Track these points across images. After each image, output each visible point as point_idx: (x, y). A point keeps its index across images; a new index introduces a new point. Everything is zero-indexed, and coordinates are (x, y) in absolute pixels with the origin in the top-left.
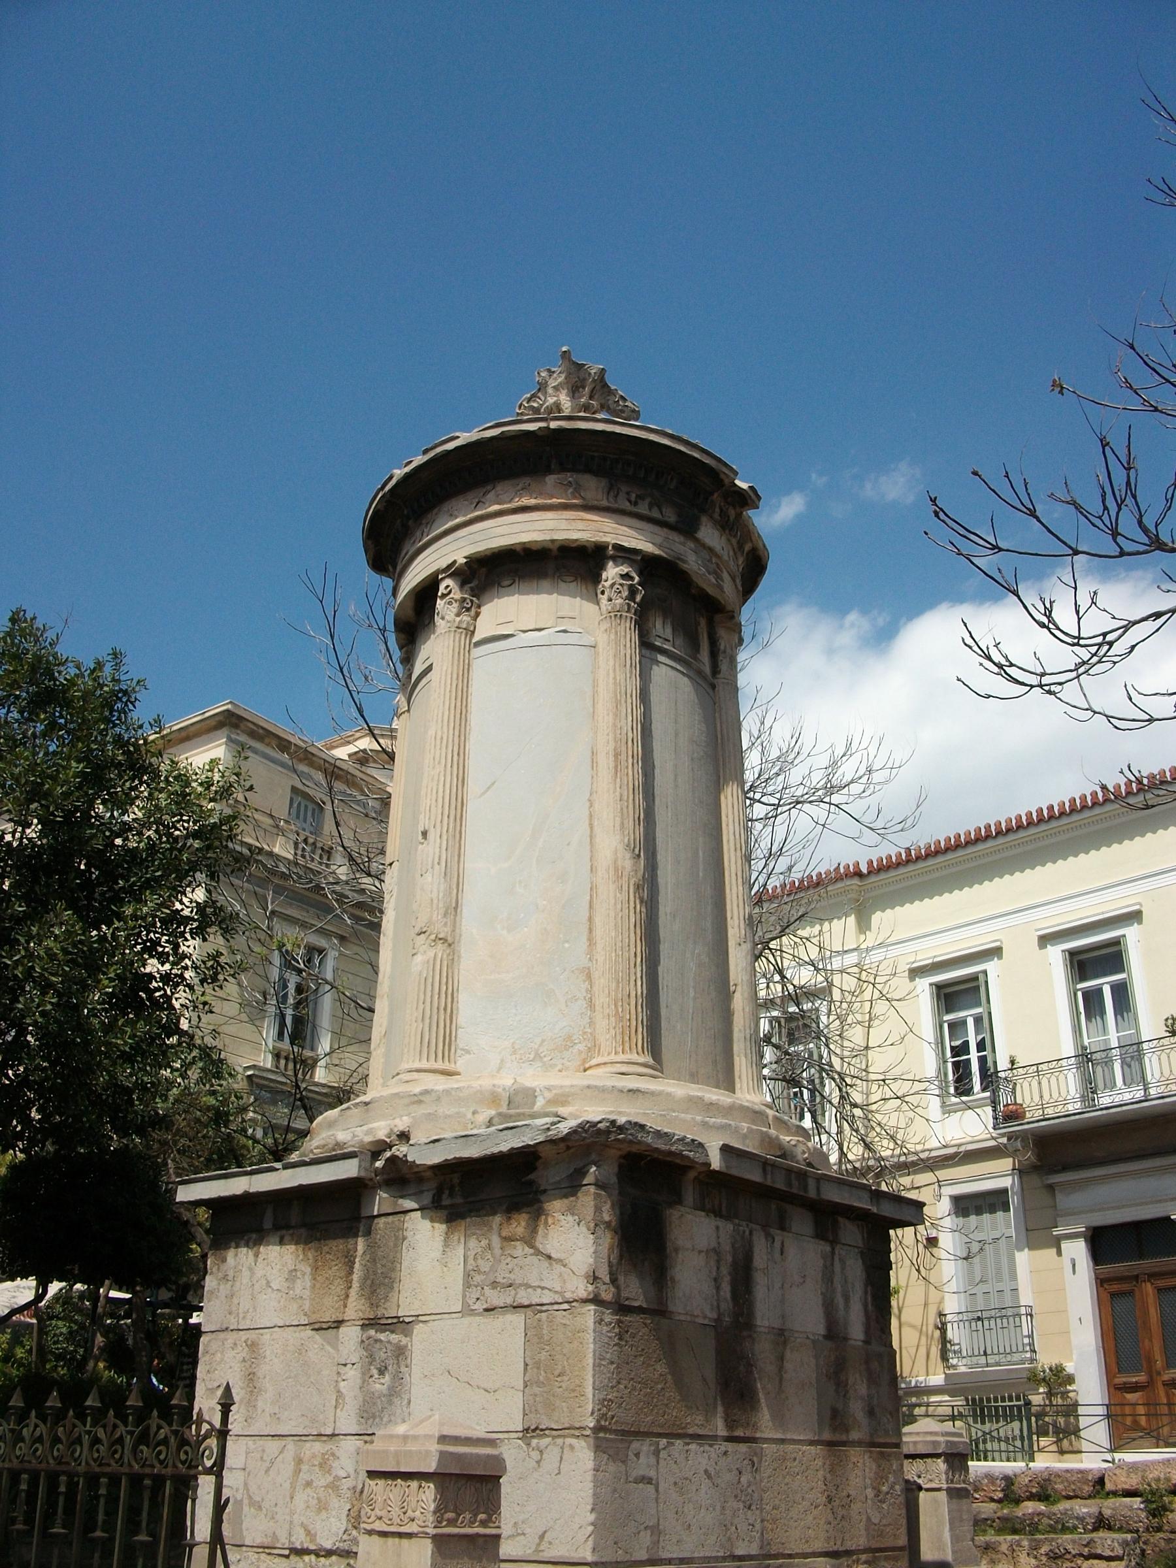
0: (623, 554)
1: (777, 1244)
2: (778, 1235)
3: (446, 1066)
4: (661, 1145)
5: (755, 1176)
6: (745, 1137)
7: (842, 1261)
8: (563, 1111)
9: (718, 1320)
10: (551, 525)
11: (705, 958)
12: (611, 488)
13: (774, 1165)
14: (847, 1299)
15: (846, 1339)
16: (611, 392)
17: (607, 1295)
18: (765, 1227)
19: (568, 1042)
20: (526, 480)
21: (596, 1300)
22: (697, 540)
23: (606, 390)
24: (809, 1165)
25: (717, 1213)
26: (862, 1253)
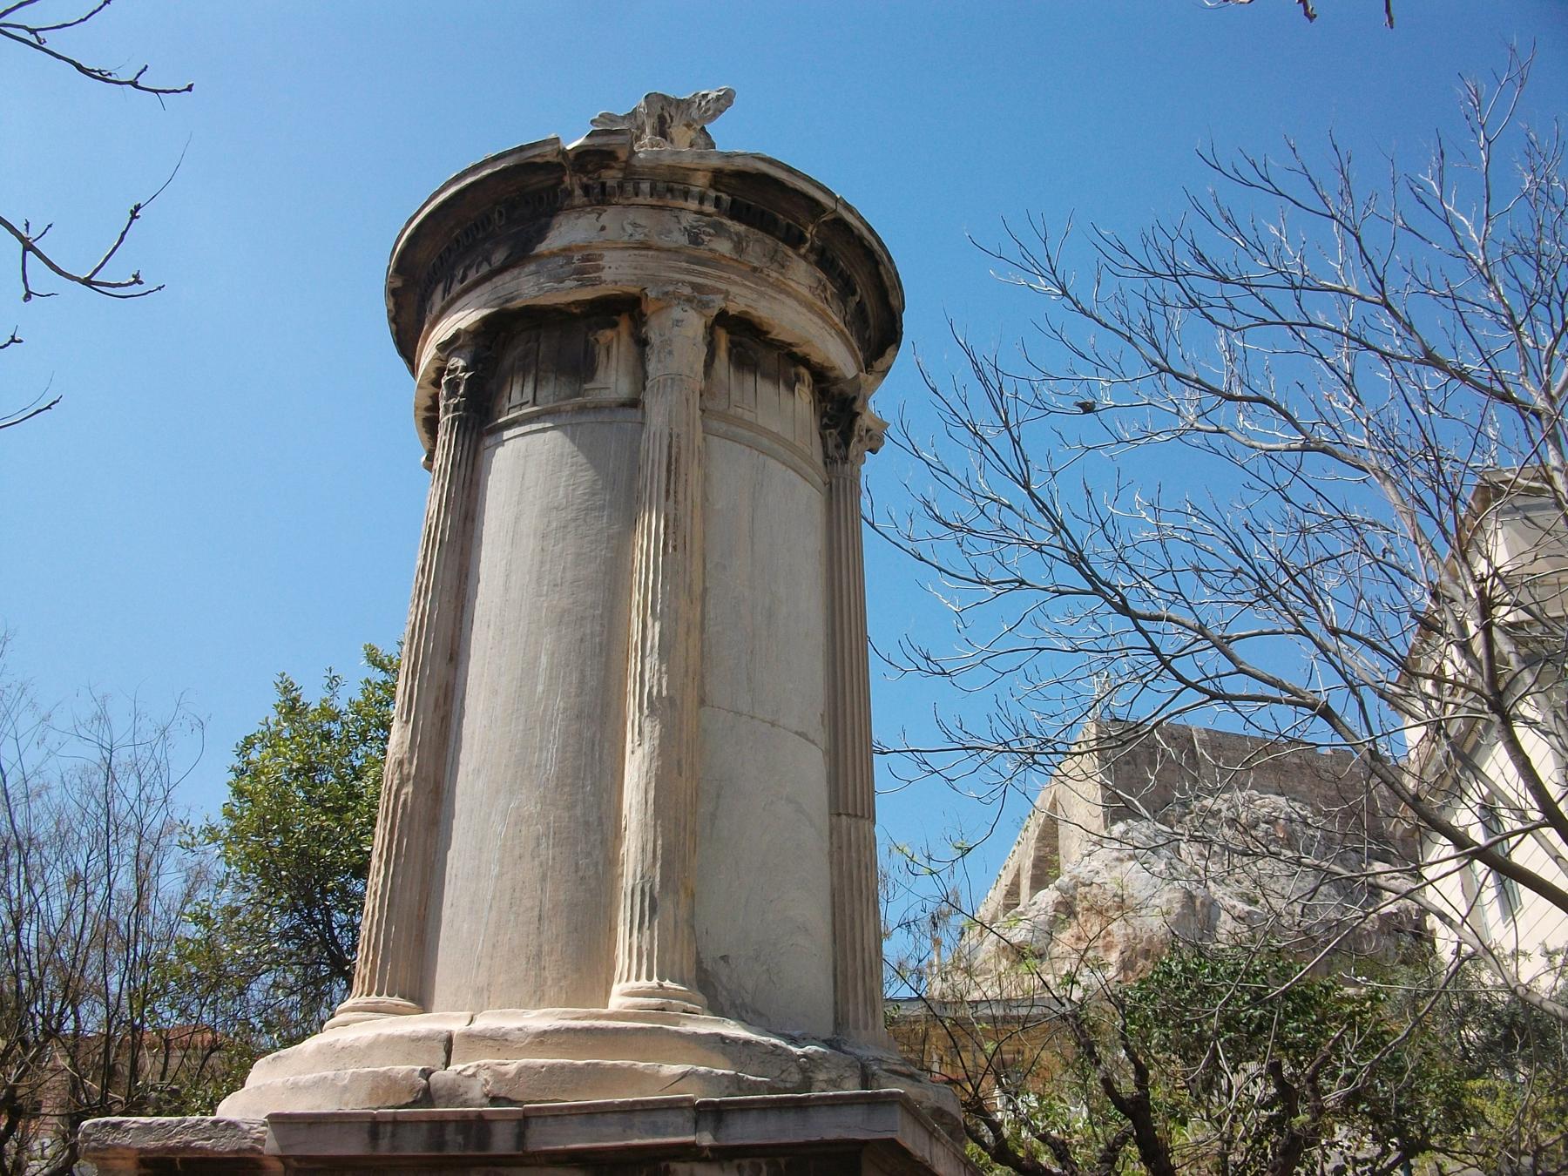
5: (354, 1146)
6: (345, 1089)
11: (532, 808)
13: (396, 1122)
16: (689, 103)
22: (539, 256)
23: (684, 106)
24: (494, 1100)
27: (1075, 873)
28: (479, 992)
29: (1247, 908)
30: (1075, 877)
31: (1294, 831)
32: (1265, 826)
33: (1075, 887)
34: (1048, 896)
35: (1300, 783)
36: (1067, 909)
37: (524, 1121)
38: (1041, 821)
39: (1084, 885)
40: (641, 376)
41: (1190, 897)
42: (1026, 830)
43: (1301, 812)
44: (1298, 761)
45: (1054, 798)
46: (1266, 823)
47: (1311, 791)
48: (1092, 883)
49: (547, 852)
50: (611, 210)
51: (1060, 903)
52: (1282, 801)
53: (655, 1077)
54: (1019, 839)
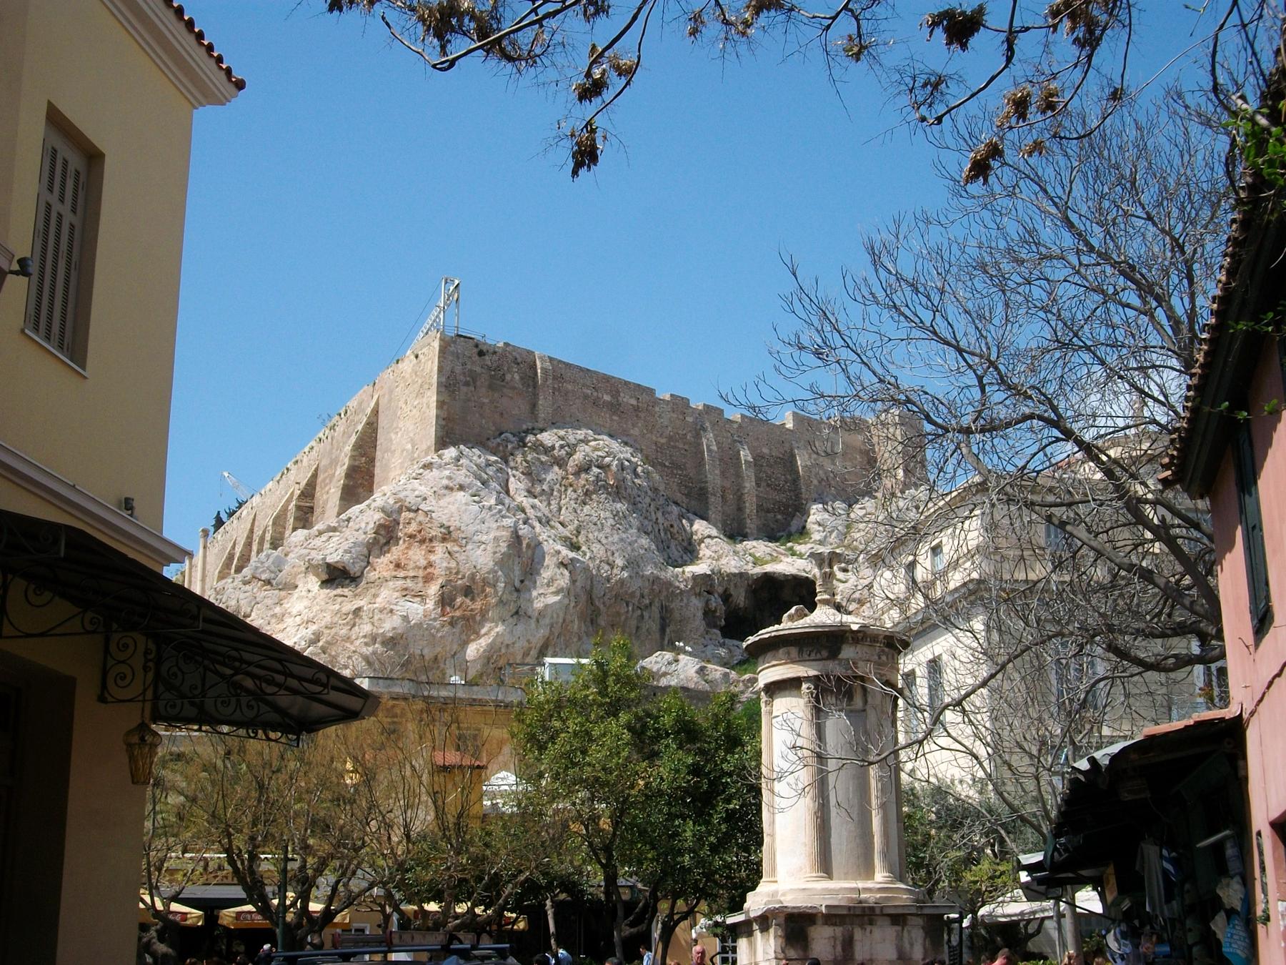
0: (808, 679)
1: (868, 930)
2: (868, 928)
3: (773, 879)
4: (796, 911)
7: (909, 932)
8: (782, 899)
9: (835, 959)
10: (781, 672)
11: (853, 829)
12: (800, 652)
14: (912, 945)
15: (910, 959)
17: (781, 956)
18: (862, 926)
19: (801, 869)
20: (774, 652)
21: (776, 958)
25: (835, 925)
26: (923, 928)
27: (401, 495)
28: (845, 874)
29: (572, 555)
30: (400, 500)
31: (624, 480)
32: (596, 470)
33: (400, 511)
34: (366, 516)
35: (634, 425)
36: (386, 535)
37: (882, 907)
38: (360, 427)
39: (409, 510)
40: (866, 702)
41: (516, 538)
42: (333, 428)
43: (633, 459)
44: (633, 402)
45: (377, 404)
46: (598, 467)
47: (643, 435)
48: (418, 509)
49: (858, 840)
50: (859, 646)
51: (381, 526)
52: (615, 445)
53: (901, 898)
54: (321, 435)
